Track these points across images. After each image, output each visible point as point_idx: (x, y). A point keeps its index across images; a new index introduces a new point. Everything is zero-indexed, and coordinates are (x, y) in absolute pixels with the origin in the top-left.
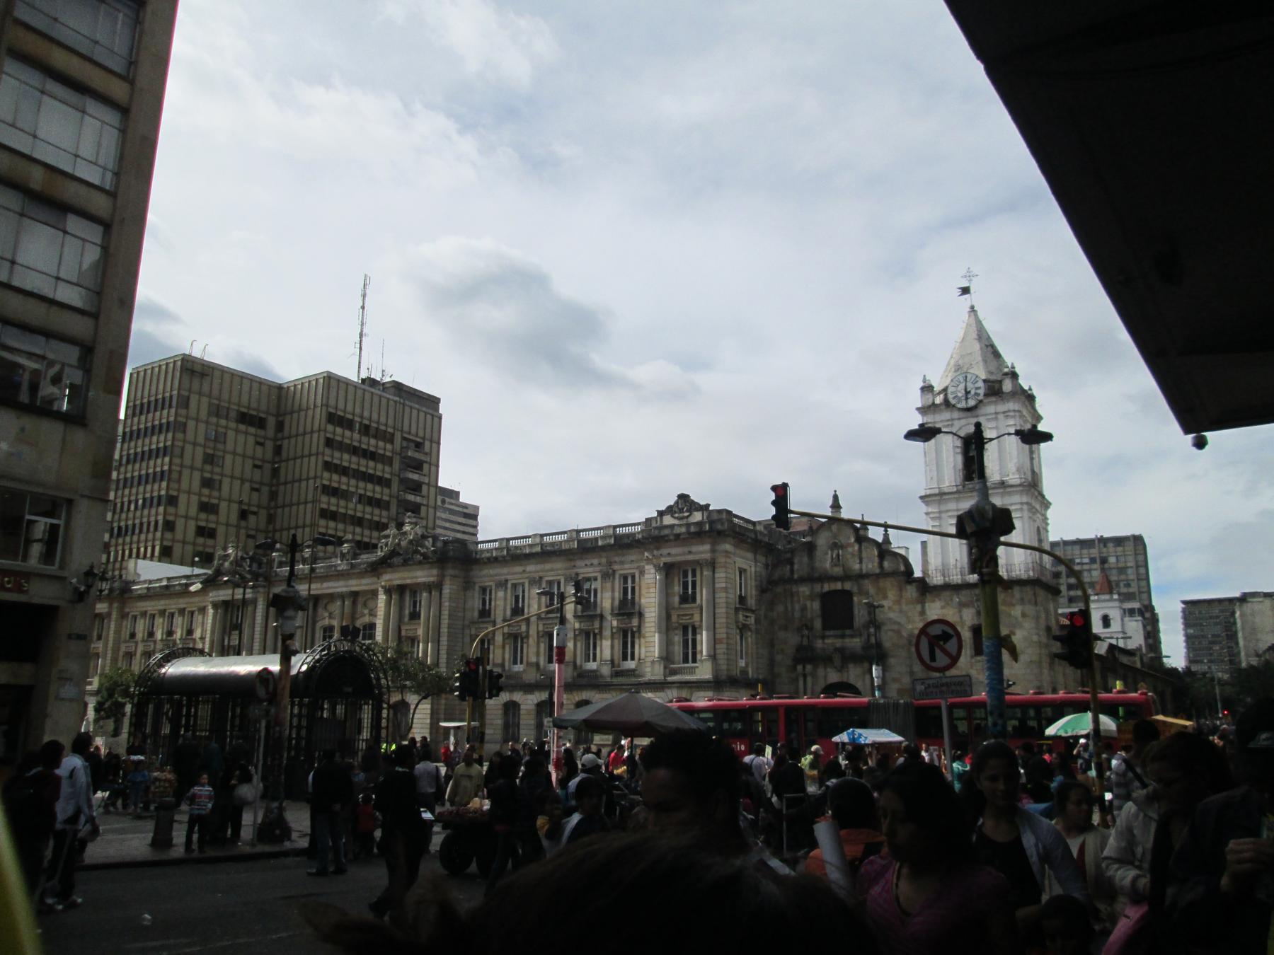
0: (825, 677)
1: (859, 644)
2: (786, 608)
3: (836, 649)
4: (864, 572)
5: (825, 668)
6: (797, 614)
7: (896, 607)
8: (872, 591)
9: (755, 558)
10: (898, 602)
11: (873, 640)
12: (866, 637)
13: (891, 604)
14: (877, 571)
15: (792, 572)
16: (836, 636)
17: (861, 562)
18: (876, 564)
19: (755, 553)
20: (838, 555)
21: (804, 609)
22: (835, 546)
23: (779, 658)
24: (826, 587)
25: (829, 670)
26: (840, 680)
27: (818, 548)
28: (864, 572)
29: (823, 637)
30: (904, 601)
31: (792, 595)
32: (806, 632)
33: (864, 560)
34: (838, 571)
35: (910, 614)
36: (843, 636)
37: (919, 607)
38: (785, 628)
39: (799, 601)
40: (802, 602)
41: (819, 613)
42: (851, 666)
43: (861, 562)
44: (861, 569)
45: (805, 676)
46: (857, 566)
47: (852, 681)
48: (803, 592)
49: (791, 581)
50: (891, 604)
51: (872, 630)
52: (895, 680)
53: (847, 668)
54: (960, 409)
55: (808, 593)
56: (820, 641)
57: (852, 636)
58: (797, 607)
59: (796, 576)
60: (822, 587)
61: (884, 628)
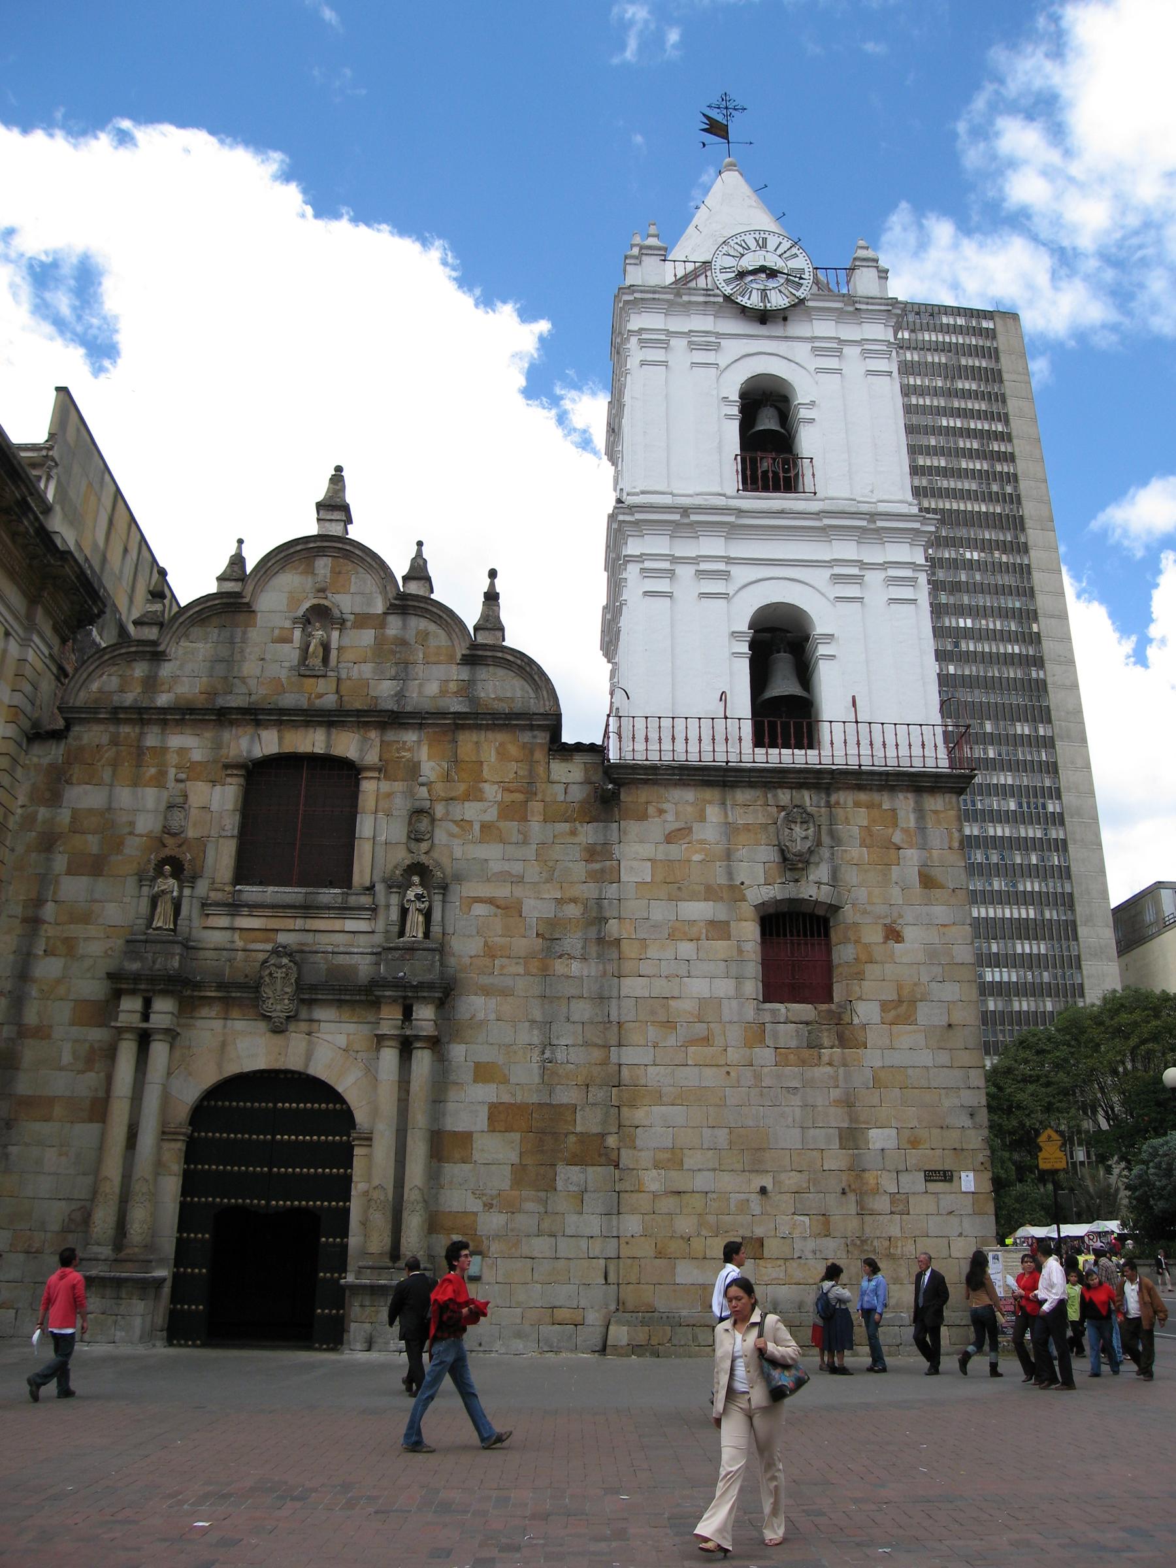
3: (277, 952)
6: (147, 824)
8: (430, 768)
9: (30, 616)
10: (515, 811)
12: (394, 915)
13: (492, 815)
14: (457, 706)
15: (151, 684)
19: (33, 600)
20: (326, 647)
21: (177, 805)
22: (320, 614)
23: (48, 968)
24: (269, 743)
29: (234, 907)
30: (536, 806)
34: (324, 694)
36: (307, 909)
37: (588, 833)
38: (95, 867)
40: (171, 784)
41: (231, 823)
45: (144, 1039)
47: (319, 1069)
48: (182, 751)
49: (142, 715)
50: (492, 815)
52: (483, 1073)
54: (745, 312)
57: (344, 910)
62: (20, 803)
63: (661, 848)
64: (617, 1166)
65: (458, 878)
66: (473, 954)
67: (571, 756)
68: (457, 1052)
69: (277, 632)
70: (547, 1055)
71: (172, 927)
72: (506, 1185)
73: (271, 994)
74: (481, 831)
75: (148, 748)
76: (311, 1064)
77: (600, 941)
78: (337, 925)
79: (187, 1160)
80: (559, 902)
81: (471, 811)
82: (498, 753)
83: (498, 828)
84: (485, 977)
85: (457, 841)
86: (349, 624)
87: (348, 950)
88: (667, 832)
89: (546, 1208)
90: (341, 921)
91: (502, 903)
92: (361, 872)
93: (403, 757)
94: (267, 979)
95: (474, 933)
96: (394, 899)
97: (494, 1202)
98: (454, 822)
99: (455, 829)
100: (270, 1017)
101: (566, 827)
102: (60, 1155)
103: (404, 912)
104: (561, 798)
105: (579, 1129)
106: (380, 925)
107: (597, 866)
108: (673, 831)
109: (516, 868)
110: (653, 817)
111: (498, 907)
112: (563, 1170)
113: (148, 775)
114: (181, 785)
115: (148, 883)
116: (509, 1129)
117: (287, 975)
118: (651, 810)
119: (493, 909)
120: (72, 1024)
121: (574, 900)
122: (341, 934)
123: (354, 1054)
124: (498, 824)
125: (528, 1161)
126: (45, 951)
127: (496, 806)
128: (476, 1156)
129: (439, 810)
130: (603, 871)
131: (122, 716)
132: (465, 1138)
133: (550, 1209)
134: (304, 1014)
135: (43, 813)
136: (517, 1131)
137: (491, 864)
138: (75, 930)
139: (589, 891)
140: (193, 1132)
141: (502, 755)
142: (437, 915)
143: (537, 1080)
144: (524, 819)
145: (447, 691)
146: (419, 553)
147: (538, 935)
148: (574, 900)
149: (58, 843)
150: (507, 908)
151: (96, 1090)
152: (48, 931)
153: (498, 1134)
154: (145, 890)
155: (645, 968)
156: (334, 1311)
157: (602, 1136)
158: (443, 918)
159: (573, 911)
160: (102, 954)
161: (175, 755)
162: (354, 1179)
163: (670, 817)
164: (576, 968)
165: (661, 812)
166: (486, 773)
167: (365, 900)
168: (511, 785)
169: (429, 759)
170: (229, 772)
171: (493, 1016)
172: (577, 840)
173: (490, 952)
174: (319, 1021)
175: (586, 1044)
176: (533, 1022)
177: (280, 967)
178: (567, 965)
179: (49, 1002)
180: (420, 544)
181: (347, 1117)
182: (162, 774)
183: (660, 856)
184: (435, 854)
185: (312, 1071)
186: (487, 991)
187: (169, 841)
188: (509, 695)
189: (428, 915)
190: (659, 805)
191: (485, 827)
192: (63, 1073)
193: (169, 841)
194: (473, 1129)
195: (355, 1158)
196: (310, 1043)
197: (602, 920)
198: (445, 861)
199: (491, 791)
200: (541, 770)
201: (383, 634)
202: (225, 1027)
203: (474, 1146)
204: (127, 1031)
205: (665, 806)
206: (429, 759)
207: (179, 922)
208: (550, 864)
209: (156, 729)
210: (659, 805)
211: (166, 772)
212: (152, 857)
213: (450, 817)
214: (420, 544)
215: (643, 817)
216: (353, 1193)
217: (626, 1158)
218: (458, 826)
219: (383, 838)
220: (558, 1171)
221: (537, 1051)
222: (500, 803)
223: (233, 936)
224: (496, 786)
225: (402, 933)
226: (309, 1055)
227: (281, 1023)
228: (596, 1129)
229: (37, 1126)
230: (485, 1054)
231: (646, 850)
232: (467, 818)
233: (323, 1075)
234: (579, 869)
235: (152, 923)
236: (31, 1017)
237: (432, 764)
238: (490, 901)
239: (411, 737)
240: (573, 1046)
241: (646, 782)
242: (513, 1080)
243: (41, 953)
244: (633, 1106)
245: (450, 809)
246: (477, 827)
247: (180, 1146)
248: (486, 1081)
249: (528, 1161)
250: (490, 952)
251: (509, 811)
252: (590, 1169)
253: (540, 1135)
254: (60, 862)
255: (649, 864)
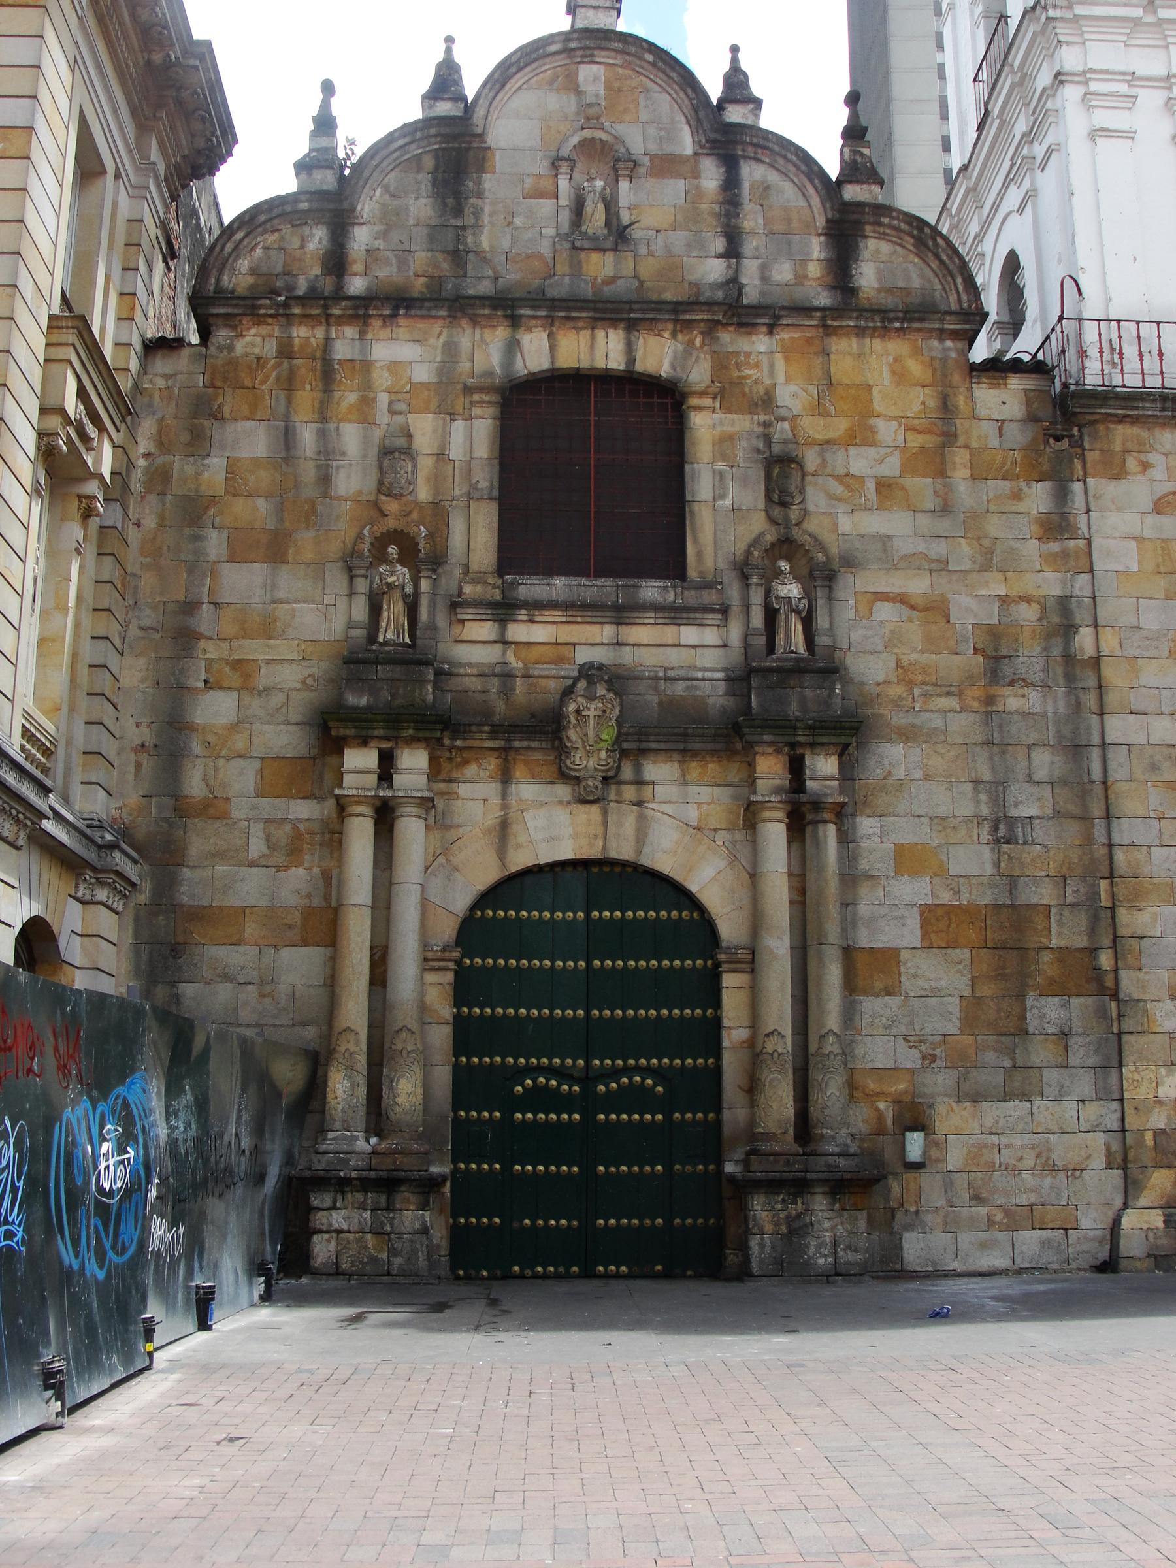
0: (503, 831)
1: (711, 659)
2: (288, 438)
4: (750, 296)
5: (506, 779)
7: (922, 486)
11: (794, 636)
12: (757, 620)
13: (891, 467)
16: (572, 608)
17: (733, 252)
18: (814, 270)
25: (526, 791)
26: (593, 852)
27: (499, 161)
28: (750, 296)
30: (960, 457)
31: (328, 375)
32: (400, 575)
33: (750, 246)
35: (994, 526)
39: (365, 411)
40: (384, 418)
41: (485, 478)
42: (659, 771)
43: (733, 252)
44: (733, 283)
46: (713, 270)
48: (394, 366)
50: (891, 467)
51: (791, 590)
53: (639, 782)
55: (422, 373)
56: (485, 630)
57: (676, 614)
58: (351, 437)
59: (356, 285)
60: (513, 347)
61: (851, 585)
62: (142, 451)
63: (1151, 520)
64: (1115, 996)
65: (849, 562)
66: (880, 679)
67: (1005, 378)
68: (866, 825)
69: (529, 182)
70: (1002, 831)
71: (407, 640)
72: (953, 1027)
73: (580, 744)
74: (878, 492)
75: (340, 362)
76: (647, 850)
77: (1069, 658)
78: (669, 633)
79: (458, 1002)
80: (1004, 601)
81: (860, 462)
82: (894, 373)
83: (903, 488)
84: (901, 715)
85: (841, 508)
86: (642, 170)
87: (690, 675)
88: (1156, 497)
89: (1014, 1060)
90: (676, 628)
91: (918, 601)
92: (699, 554)
93: (745, 377)
94: (573, 720)
95: (880, 648)
96: (757, 597)
97: (938, 1052)
98: (837, 477)
99: (838, 489)
100: (577, 778)
101: (1006, 486)
102: (262, 996)
103: (771, 615)
104: (994, 442)
105: (1055, 942)
106: (735, 633)
107: (1054, 547)
108: (1164, 496)
109: (938, 549)
110: (1135, 474)
111: (913, 608)
112: (1036, 1003)
113: (344, 405)
114: (399, 419)
115: (363, 572)
116: (952, 944)
117: (604, 711)
118: (1132, 463)
119: (905, 611)
120: (260, 794)
121: (1027, 599)
122: (675, 649)
123: (711, 835)
124: (902, 481)
125: (986, 990)
126: (206, 682)
127: (897, 453)
128: (908, 985)
129: (811, 459)
130: (1065, 554)
131: (297, 311)
132: (888, 959)
133: (1020, 1063)
134: (627, 772)
135: (181, 466)
136: (965, 947)
137: (897, 542)
138: (254, 649)
139: (1051, 585)
140: (462, 957)
141: (900, 376)
142: (822, 621)
143: (989, 870)
144: (941, 473)
145: (806, 277)
146: (735, 61)
147: (976, 650)
148: (1027, 599)
149: (211, 513)
150: (927, 609)
151: (309, 895)
152: (210, 650)
153: (935, 950)
154: (362, 585)
155: (1137, 700)
156: (689, 1221)
157: (1093, 952)
158: (831, 623)
159: (1027, 614)
160: (299, 686)
161: (386, 374)
162: (726, 1022)
163: (1158, 473)
164: (1034, 700)
165: (1145, 466)
166: (878, 405)
167: (709, 597)
168: (917, 422)
169: (789, 380)
170: (476, 397)
171: (918, 774)
172: (1021, 507)
173: (905, 674)
174: (653, 783)
175: (1058, 815)
176: (977, 782)
177: (591, 698)
178: (1023, 696)
179: (221, 762)
180: (735, 50)
181: (706, 926)
182: (367, 402)
183: (1148, 533)
184: (811, 525)
185: (645, 861)
186: (908, 735)
187: (392, 506)
188: (901, 284)
189: (808, 622)
190: (1142, 457)
191: (884, 487)
192: (254, 870)
193: (392, 506)
194: (899, 944)
195: (724, 991)
196: (642, 819)
197: (1068, 629)
198: (828, 538)
199: (887, 431)
200: (961, 401)
201: (698, 187)
202: (504, 796)
203: (903, 970)
204: (359, 803)
205: (1153, 458)
206: (789, 380)
207: (418, 633)
208: (986, 543)
209: (350, 332)
210: (1142, 457)
211: (374, 400)
212: (366, 532)
213: (828, 471)
214: (735, 50)
215: (1120, 473)
216: (726, 1043)
217: (1129, 983)
218: (842, 483)
219: (728, 502)
220: (1029, 1005)
221: (987, 826)
222: (903, 450)
223: (504, 653)
224: (895, 423)
225: (771, 647)
226: (641, 838)
227: (597, 788)
228: (1081, 942)
229: (221, 952)
230: (908, 832)
231: (1129, 522)
232: (854, 470)
233: (665, 864)
234: (1032, 549)
235: (377, 636)
236: (194, 785)
237: (793, 388)
238: (902, 599)
239: (760, 343)
240: (1038, 817)
241: (1121, 420)
242: (954, 870)
243: (201, 685)
244: (1133, 907)
245: (828, 456)
246: (871, 486)
247: (449, 977)
248: (914, 873)
249: (986, 990)
250: (905, 674)
251: (913, 462)
252: (1075, 1001)
253: (1001, 952)
254: (215, 543)
255: (1133, 544)
